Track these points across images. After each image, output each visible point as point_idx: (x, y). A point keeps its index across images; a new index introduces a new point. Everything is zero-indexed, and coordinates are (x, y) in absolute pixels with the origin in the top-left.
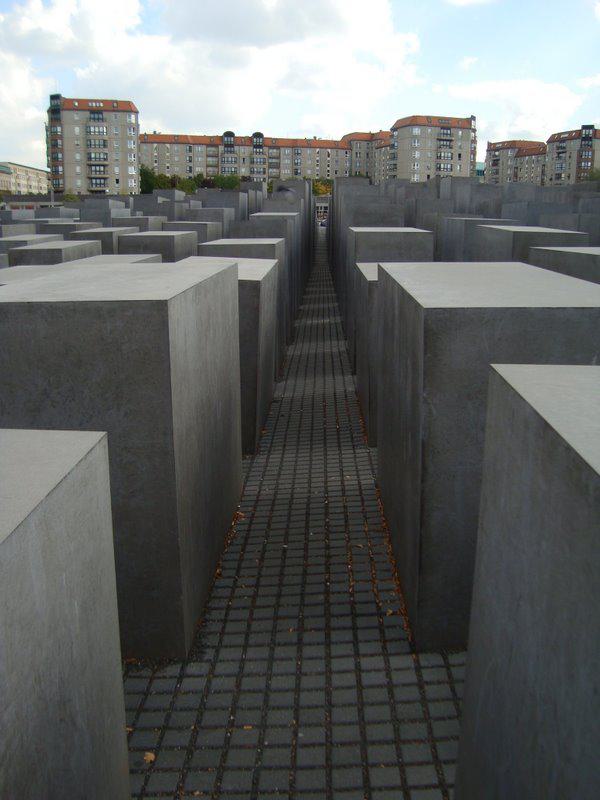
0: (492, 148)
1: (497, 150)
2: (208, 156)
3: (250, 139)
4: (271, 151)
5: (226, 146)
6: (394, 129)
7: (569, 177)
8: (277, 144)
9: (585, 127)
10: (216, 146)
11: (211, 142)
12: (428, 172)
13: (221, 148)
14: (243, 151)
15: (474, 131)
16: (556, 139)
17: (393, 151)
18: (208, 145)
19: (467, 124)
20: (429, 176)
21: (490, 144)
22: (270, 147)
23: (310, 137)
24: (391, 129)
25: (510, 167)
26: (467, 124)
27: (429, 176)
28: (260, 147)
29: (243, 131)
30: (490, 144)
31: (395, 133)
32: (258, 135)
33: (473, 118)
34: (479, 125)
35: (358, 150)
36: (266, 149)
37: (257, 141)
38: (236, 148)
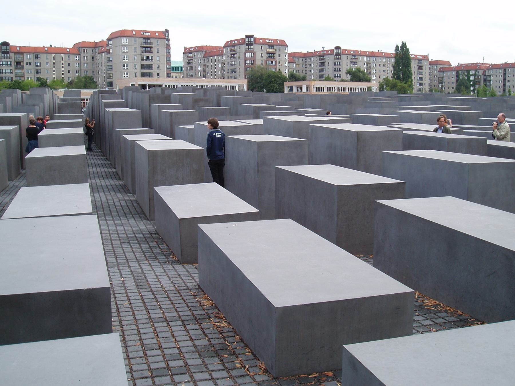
0: (187, 52)
1: (190, 53)
4: (16, 56)
6: (109, 40)
8: (21, 51)
9: (247, 36)
12: (136, 71)
15: (168, 40)
16: (231, 45)
17: (108, 56)
19: (164, 35)
21: (185, 48)
26: (164, 35)
28: (7, 53)
30: (185, 48)
31: (110, 42)
33: (167, 31)
34: (171, 36)
35: (86, 55)
36: (12, 55)
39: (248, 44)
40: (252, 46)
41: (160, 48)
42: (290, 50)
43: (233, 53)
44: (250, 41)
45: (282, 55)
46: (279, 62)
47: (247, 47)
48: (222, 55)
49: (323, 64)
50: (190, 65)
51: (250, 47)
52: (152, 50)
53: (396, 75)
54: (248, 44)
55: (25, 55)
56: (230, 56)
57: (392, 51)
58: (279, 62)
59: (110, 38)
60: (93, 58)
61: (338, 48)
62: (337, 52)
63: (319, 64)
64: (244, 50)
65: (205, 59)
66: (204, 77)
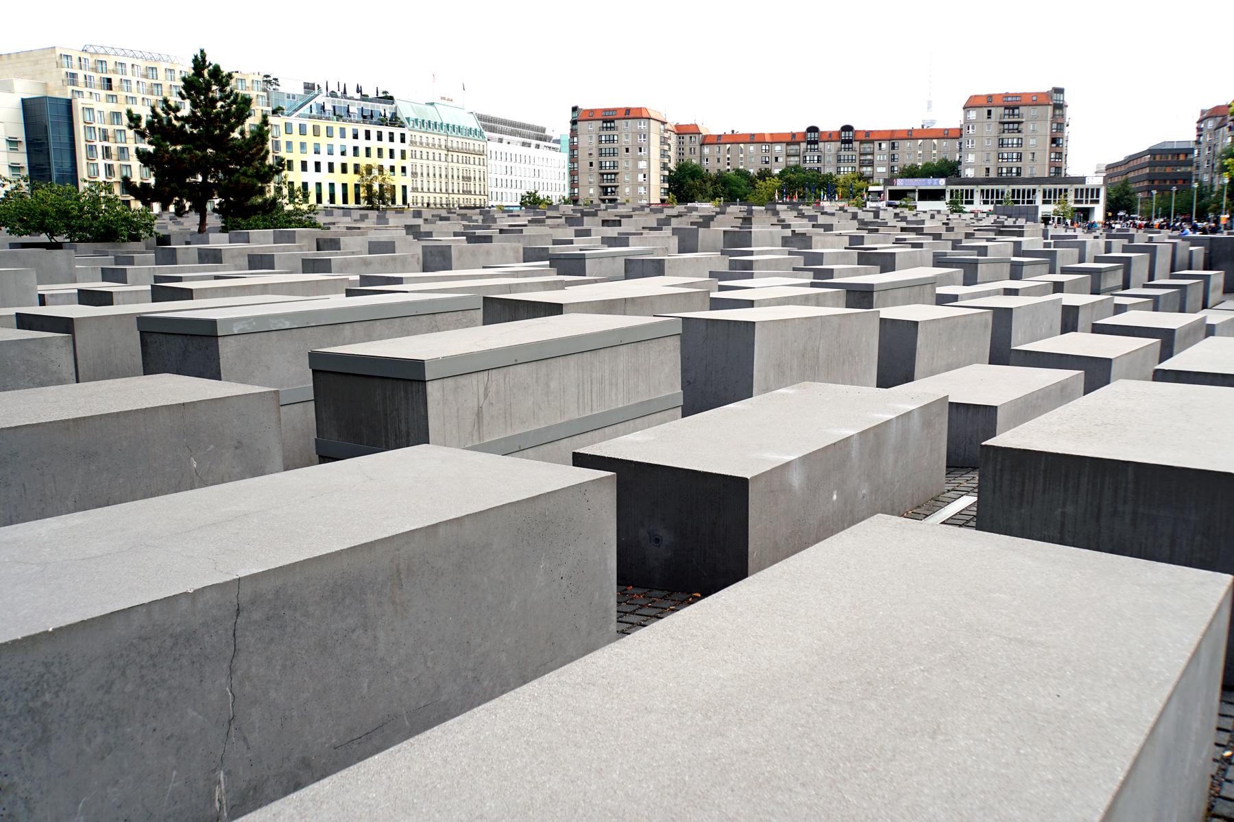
2: (788, 156)
3: (839, 133)
4: (866, 145)
5: (809, 143)
8: (869, 138)
10: (798, 143)
11: (792, 140)
13: (803, 145)
14: (830, 148)
18: (788, 144)
20: (988, 170)
22: (862, 142)
23: (918, 126)
27: (988, 170)
28: (850, 142)
29: (830, 124)
32: (847, 128)
36: (856, 144)
37: (847, 136)
38: (821, 145)
52: (1021, 126)
55: (876, 144)
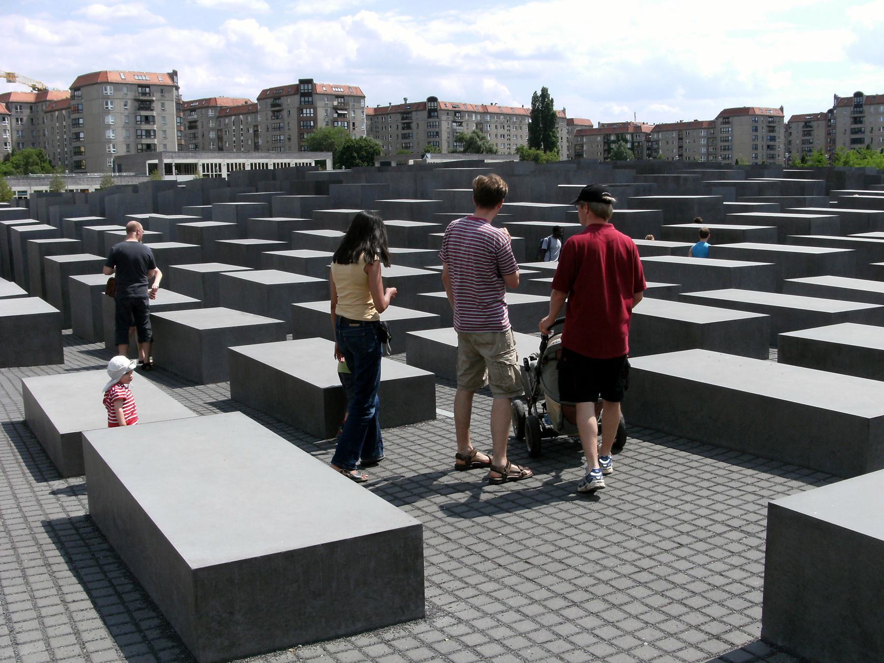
6: (75, 88)
7: (289, 139)
24: (71, 89)
25: (212, 129)
39: (304, 95)
40: (310, 99)
41: (166, 103)
42: (371, 102)
43: (277, 108)
44: (305, 90)
45: (359, 112)
46: (354, 124)
47: (303, 99)
48: (255, 112)
49: (408, 126)
50: (193, 131)
51: (306, 99)
53: (534, 141)
54: (304, 95)
56: (270, 114)
57: (529, 106)
58: (354, 124)
59: (78, 85)
60: (32, 120)
61: (433, 99)
62: (431, 107)
63: (400, 126)
64: (297, 105)
65: (222, 119)
66: (221, 149)
